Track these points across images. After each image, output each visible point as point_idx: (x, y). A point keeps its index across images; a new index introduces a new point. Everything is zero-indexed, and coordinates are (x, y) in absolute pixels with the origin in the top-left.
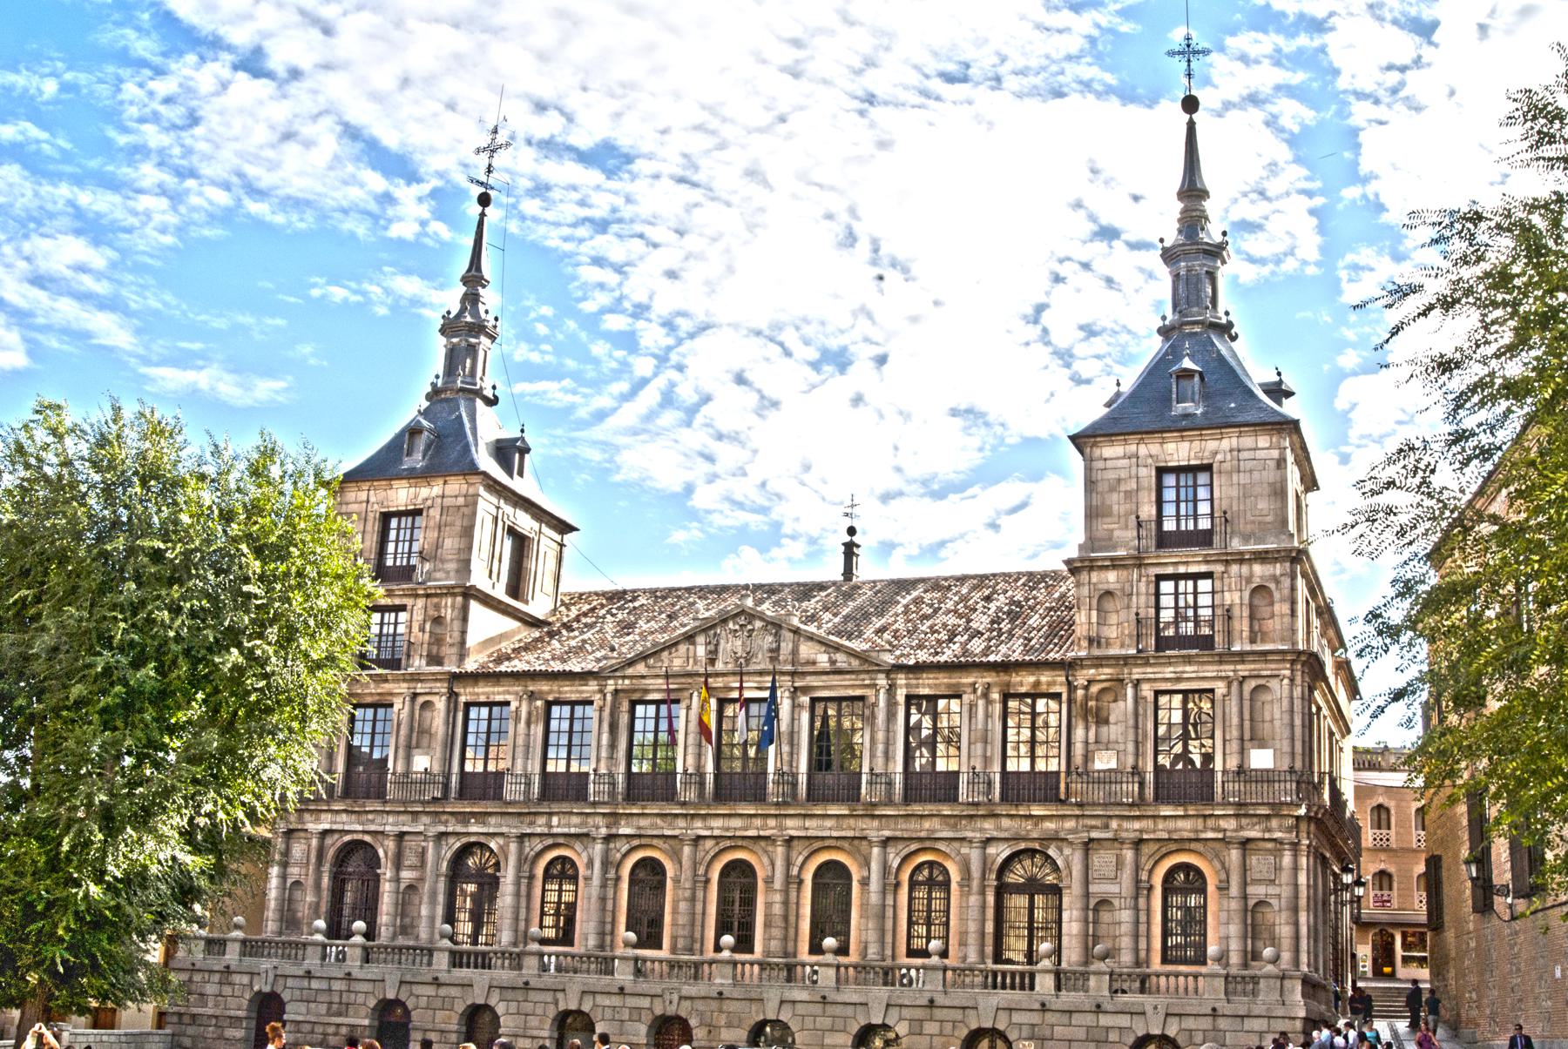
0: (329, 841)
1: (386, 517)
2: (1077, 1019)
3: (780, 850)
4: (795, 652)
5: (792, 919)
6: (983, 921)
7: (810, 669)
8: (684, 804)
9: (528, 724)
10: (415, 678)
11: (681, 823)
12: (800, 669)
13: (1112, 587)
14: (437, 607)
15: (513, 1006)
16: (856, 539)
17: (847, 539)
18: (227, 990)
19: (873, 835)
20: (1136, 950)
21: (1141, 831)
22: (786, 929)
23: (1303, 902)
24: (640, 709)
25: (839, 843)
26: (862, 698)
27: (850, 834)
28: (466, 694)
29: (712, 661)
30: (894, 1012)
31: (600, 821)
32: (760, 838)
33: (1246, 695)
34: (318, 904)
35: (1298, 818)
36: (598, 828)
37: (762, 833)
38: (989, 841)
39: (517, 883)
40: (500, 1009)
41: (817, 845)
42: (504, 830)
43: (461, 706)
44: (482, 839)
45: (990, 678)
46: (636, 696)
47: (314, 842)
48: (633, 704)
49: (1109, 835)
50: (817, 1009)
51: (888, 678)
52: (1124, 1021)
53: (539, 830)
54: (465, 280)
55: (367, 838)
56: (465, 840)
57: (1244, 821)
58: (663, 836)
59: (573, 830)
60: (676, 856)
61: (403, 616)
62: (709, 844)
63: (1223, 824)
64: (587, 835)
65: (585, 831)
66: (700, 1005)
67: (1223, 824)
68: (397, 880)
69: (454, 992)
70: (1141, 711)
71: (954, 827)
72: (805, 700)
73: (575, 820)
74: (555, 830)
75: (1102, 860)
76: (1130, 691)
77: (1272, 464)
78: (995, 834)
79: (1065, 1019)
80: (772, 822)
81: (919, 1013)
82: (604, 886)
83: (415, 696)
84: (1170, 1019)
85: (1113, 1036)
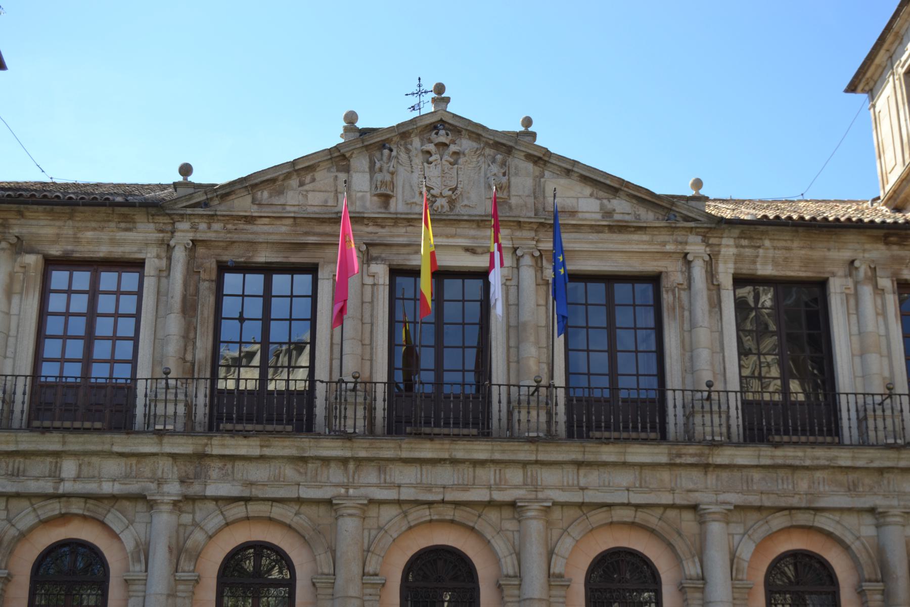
3: (535, 527)
4: (538, 191)
11: (336, 474)
24: (232, 281)
25: (641, 517)
26: (655, 279)
29: (386, 198)
31: (164, 467)
32: (491, 504)
36: (160, 482)
37: (498, 496)
41: (599, 517)
46: (228, 257)
51: (705, 241)
53: (33, 486)
58: (299, 501)
59: (107, 488)
60: (321, 539)
62: (388, 513)
64: (139, 498)
65: (134, 488)
71: (852, 489)
73: (112, 467)
74: (66, 487)
80: (515, 476)
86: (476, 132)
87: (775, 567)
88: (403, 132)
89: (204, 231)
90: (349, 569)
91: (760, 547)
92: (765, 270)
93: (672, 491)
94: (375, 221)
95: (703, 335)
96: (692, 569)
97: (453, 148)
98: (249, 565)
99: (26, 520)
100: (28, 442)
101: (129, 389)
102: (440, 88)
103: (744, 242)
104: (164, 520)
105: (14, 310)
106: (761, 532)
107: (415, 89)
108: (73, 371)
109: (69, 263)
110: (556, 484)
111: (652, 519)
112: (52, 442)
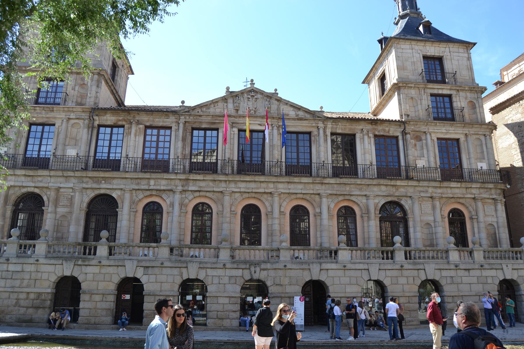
0: (11, 192)
3: (276, 199)
4: (278, 109)
9: (135, 135)
11: (223, 185)
13: (413, 96)
15: (152, 278)
24: (195, 132)
25: (305, 196)
26: (309, 133)
29: (237, 110)
31: (178, 182)
32: (265, 193)
34: (3, 226)
37: (267, 191)
40: (144, 280)
41: (294, 196)
42: (122, 187)
44: (108, 192)
46: (194, 126)
50: (340, 273)
51: (323, 123)
52: (493, 273)
53: (143, 187)
55: (37, 191)
56: (97, 192)
57: (482, 191)
58: (214, 191)
59: (162, 188)
62: (237, 195)
63: (474, 191)
64: (171, 190)
65: (169, 188)
67: (474, 191)
69: (111, 270)
71: (360, 190)
73: (164, 182)
77: (465, 59)
79: (466, 273)
80: (271, 185)
81: (395, 273)
85: (490, 281)
86: (262, 93)
87: (340, 210)
88: (242, 92)
89: (188, 119)
90: (227, 210)
91: (336, 205)
92: (339, 131)
93: (313, 190)
94: (234, 117)
95: (322, 149)
96: (318, 210)
97: (256, 97)
98: (200, 209)
99: (141, 196)
100: (141, 175)
101: (168, 162)
102: (252, 81)
103: (334, 124)
104: (178, 196)
105: (137, 140)
106: (336, 201)
107: (245, 81)
108: (153, 156)
110: (282, 188)
111: (307, 197)
112: (147, 175)
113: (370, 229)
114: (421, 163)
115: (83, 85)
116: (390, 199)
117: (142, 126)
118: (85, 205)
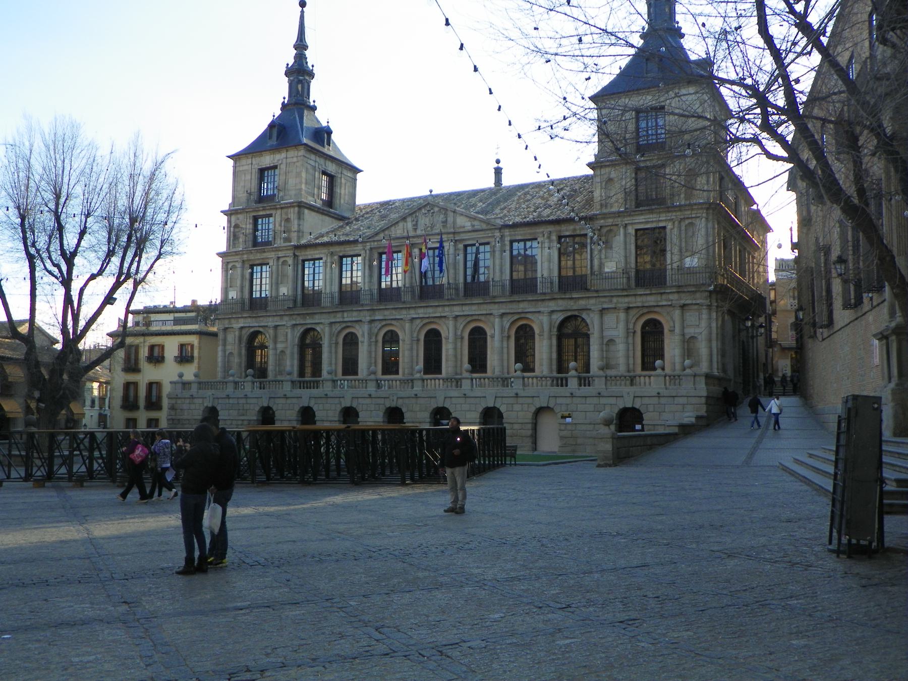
0: (244, 332)
1: (262, 171)
2: (589, 400)
4: (454, 222)
5: (459, 357)
6: (551, 352)
7: (462, 230)
8: (404, 302)
10: (278, 249)
11: (404, 312)
12: (457, 230)
14: (287, 214)
16: (500, 165)
17: (496, 165)
18: (193, 407)
19: (495, 312)
20: (628, 365)
21: (628, 303)
22: (456, 361)
23: (714, 336)
27: (484, 312)
28: (302, 255)
29: (415, 230)
30: (499, 400)
32: (441, 317)
33: (683, 228)
34: (241, 363)
35: (710, 292)
37: (443, 315)
38: (553, 312)
39: (330, 347)
41: (469, 319)
43: (300, 262)
44: (313, 326)
45: (551, 228)
46: (381, 250)
47: (237, 333)
48: (381, 254)
49: (613, 306)
50: (462, 400)
53: (338, 320)
54: (296, 47)
56: (305, 327)
57: (683, 295)
59: (354, 319)
61: (271, 219)
63: (671, 297)
66: (407, 401)
68: (275, 349)
69: (294, 401)
70: (628, 240)
72: (461, 246)
73: (355, 314)
74: (346, 320)
75: (610, 319)
76: (622, 230)
78: (555, 308)
79: (583, 400)
80: (447, 309)
82: (370, 345)
83: (278, 258)
84: (636, 399)
94: (413, 237)
109: (347, 256)
110: (457, 311)
113: (544, 351)
114: (610, 267)
115: (288, 220)
116: (569, 314)
117: (336, 257)
118: (297, 340)
